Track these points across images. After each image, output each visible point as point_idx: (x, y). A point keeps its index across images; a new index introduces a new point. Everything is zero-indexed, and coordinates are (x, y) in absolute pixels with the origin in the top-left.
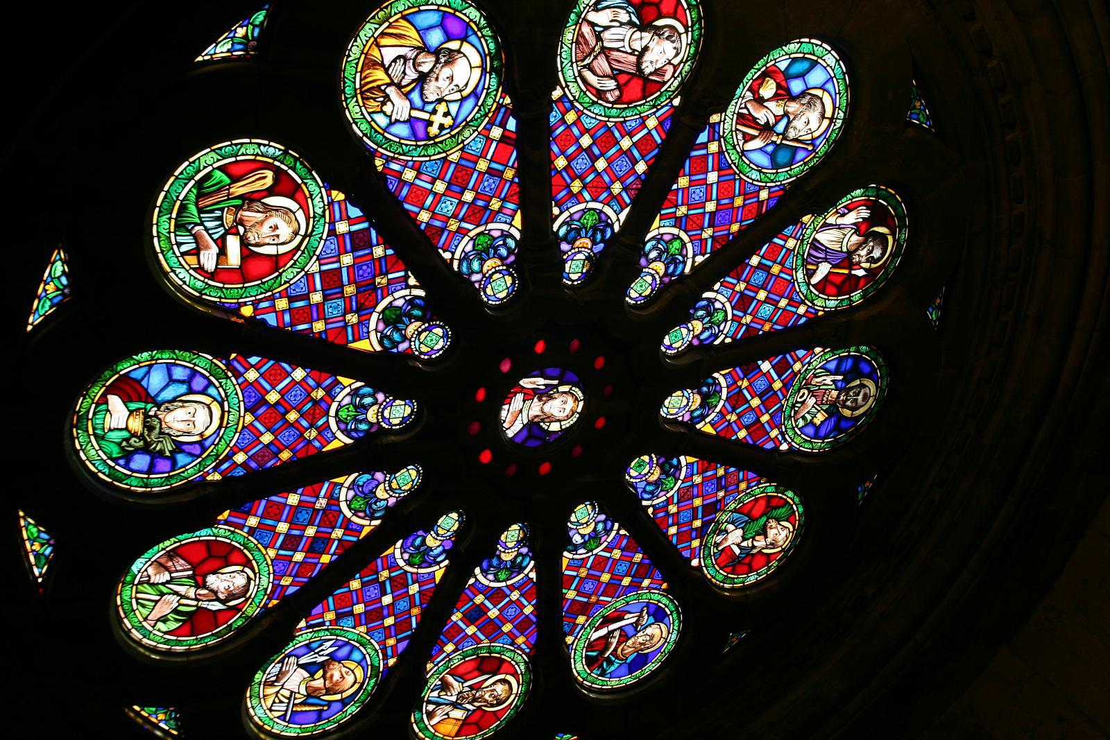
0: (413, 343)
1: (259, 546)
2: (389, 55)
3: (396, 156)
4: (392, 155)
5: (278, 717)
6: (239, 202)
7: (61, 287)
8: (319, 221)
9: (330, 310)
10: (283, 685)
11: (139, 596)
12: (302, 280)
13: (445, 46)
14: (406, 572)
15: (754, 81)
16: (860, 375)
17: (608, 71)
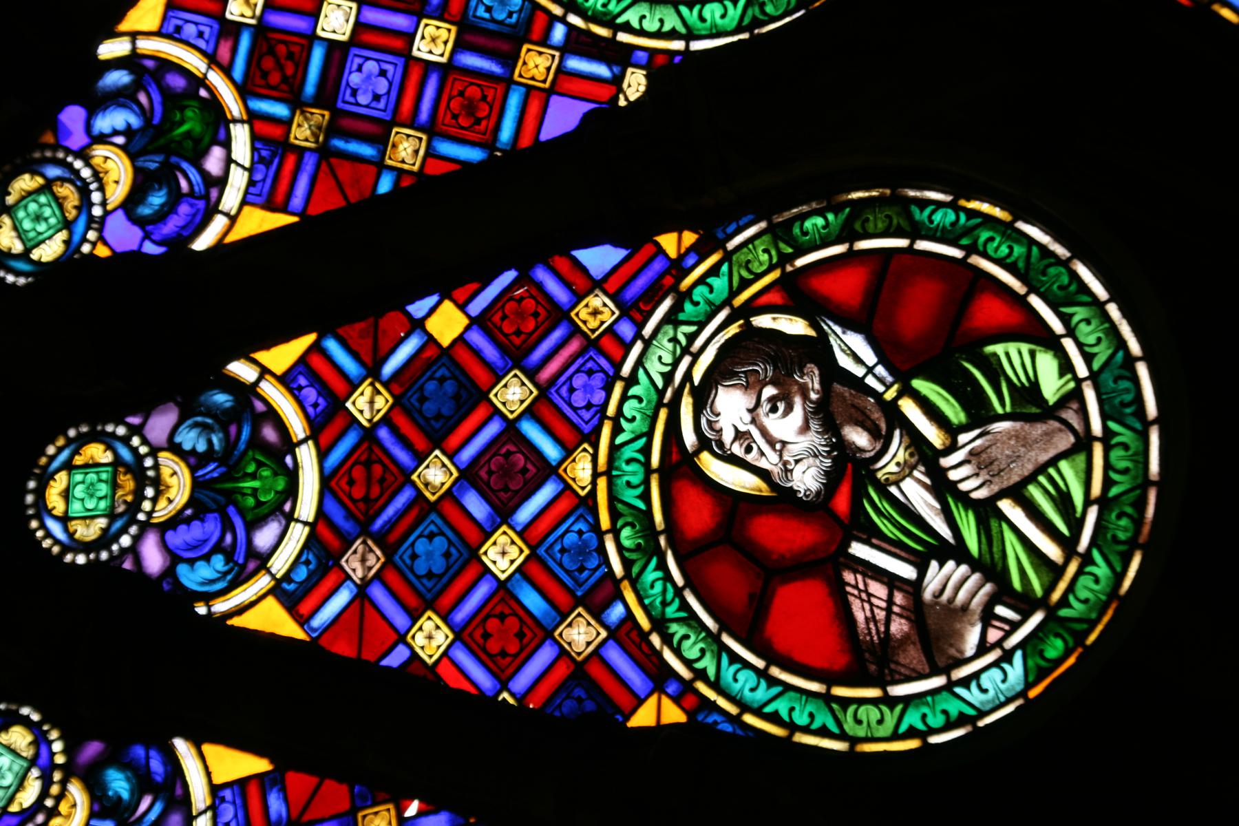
11: (1053, 551)
14: (245, 91)
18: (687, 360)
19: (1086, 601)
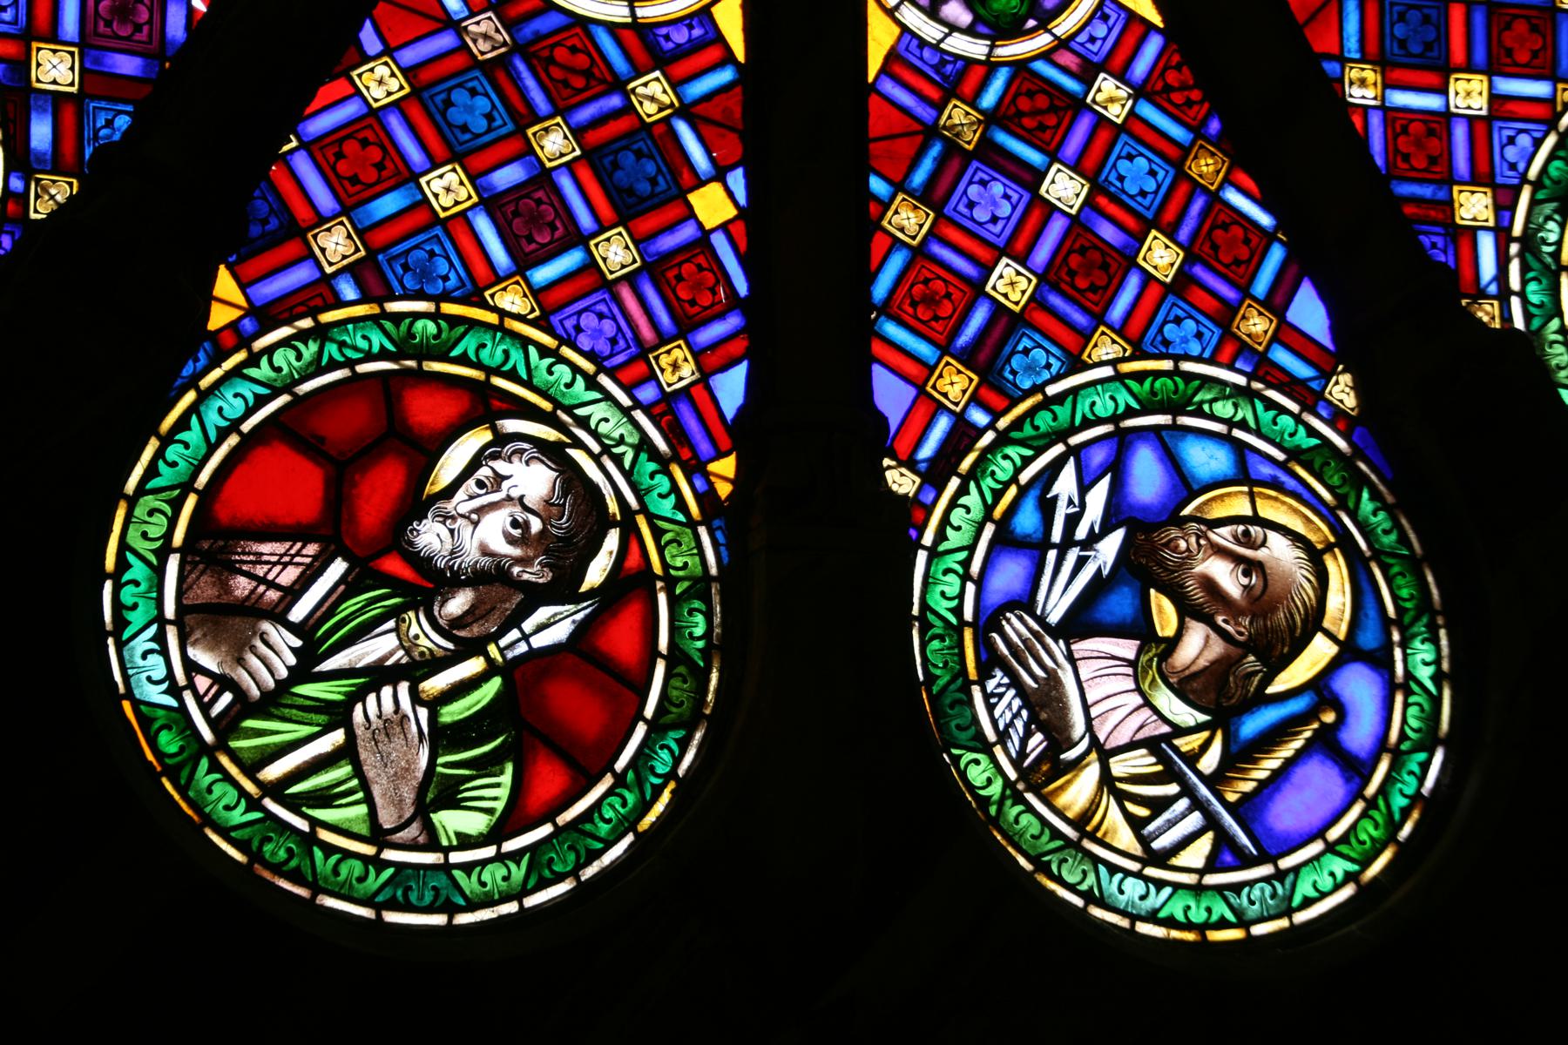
1: (449, 308)
5: (1213, 865)
11: (273, 772)
14: (1020, 67)
18: (596, 449)
19: (210, 791)
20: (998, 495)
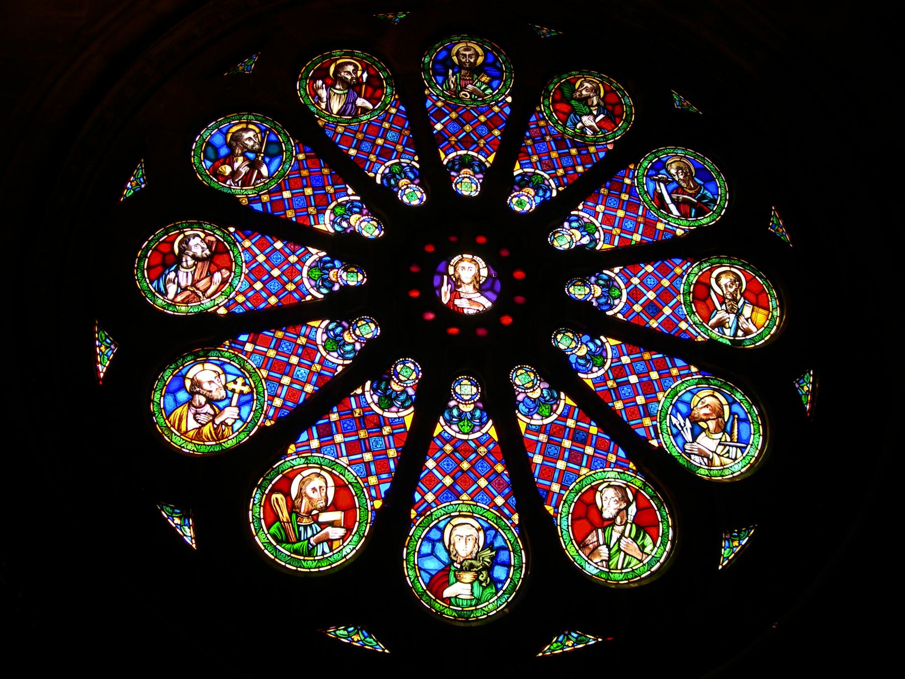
0: (409, 385)
1: (577, 481)
2: (193, 424)
3: (264, 412)
4: (263, 416)
5: (742, 453)
6: (294, 516)
7: (356, 631)
8: (310, 460)
9: (379, 446)
10: (712, 452)
11: (619, 567)
12: (353, 468)
13: (188, 389)
14: (610, 367)
15: (219, 181)
16: (449, 57)
17: (207, 279)
20: (667, 431)
